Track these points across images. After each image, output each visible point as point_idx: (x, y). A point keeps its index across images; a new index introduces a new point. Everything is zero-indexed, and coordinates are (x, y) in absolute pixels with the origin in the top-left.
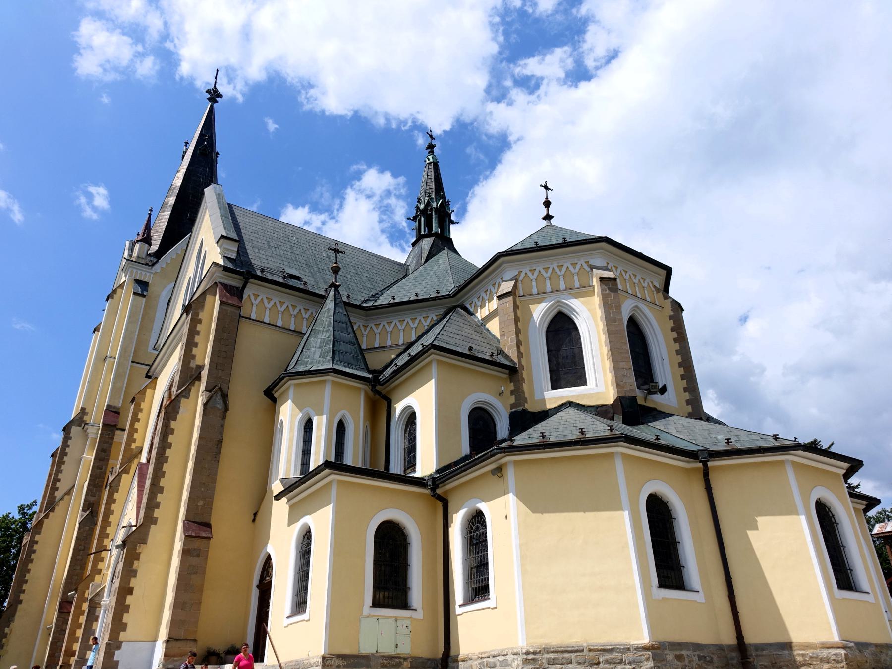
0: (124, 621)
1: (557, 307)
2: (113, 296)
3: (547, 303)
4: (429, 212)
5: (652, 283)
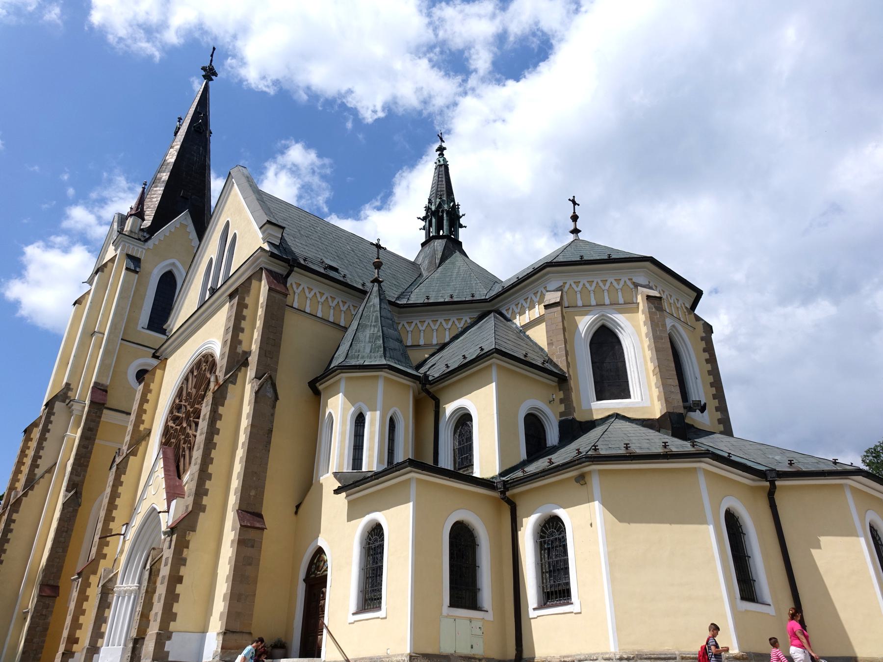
0: (174, 610)
1: (601, 320)
2: (103, 269)
3: (592, 316)
4: (440, 214)
5: (684, 304)
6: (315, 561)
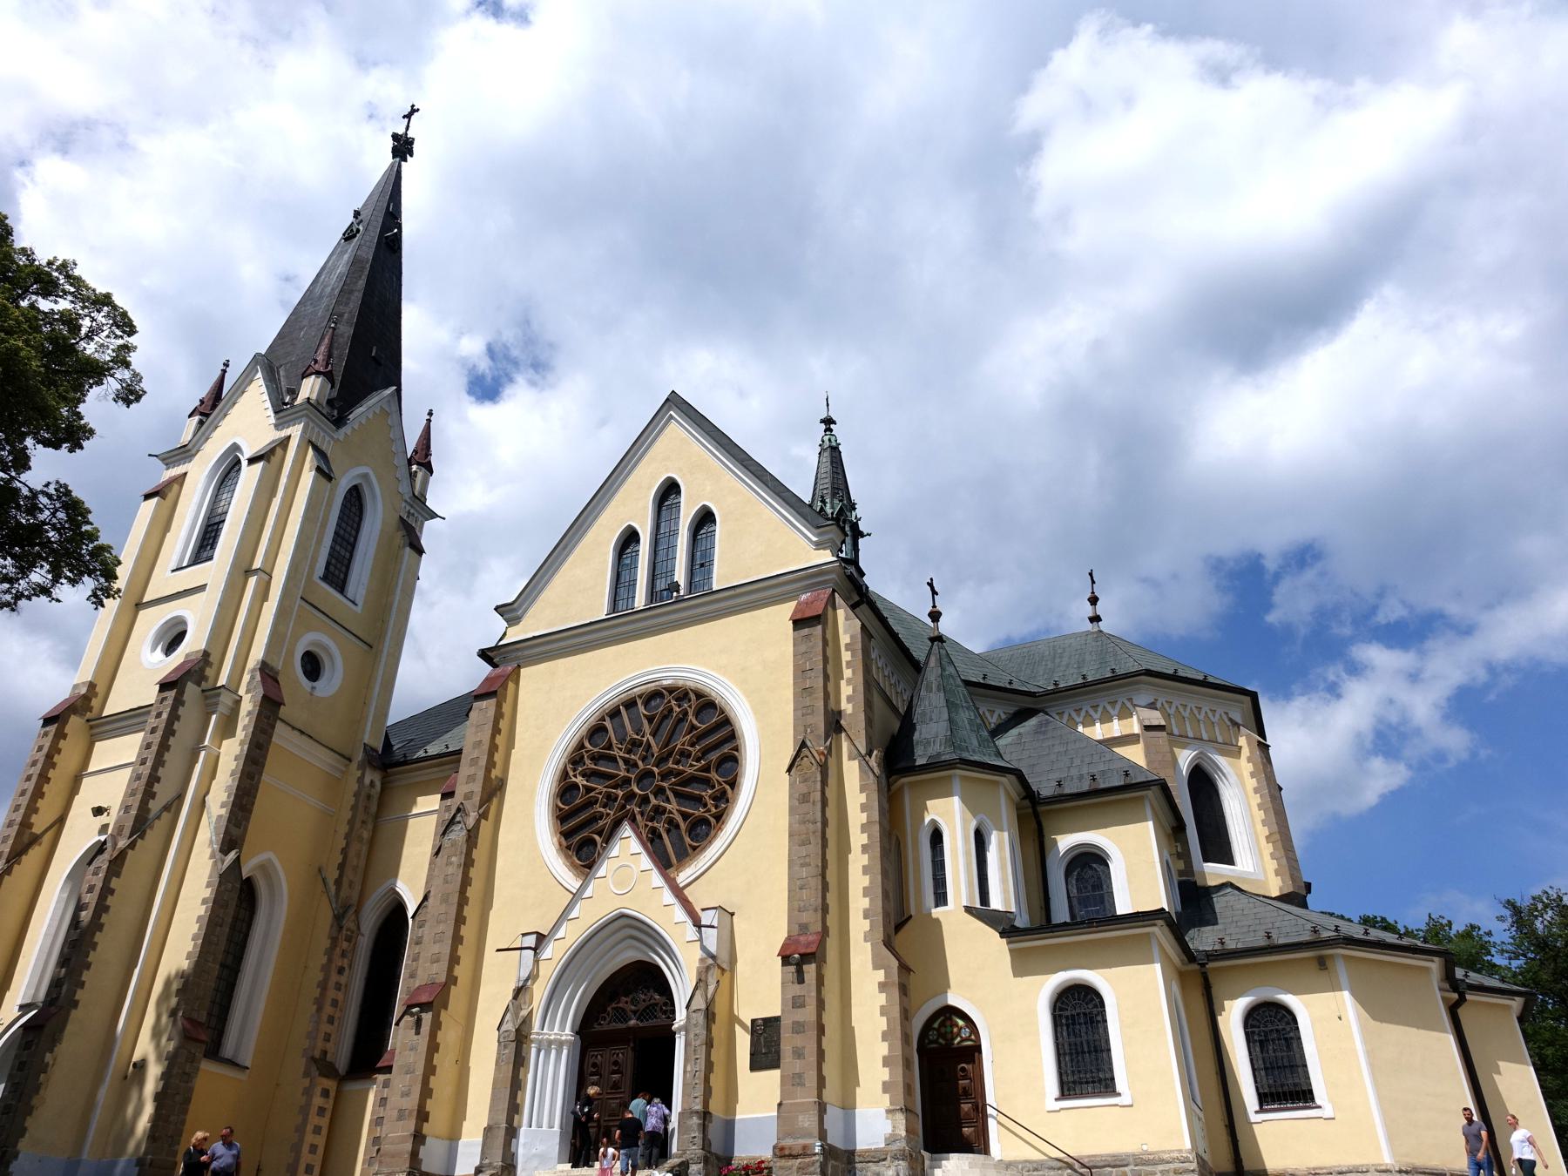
6: (936, 1025)
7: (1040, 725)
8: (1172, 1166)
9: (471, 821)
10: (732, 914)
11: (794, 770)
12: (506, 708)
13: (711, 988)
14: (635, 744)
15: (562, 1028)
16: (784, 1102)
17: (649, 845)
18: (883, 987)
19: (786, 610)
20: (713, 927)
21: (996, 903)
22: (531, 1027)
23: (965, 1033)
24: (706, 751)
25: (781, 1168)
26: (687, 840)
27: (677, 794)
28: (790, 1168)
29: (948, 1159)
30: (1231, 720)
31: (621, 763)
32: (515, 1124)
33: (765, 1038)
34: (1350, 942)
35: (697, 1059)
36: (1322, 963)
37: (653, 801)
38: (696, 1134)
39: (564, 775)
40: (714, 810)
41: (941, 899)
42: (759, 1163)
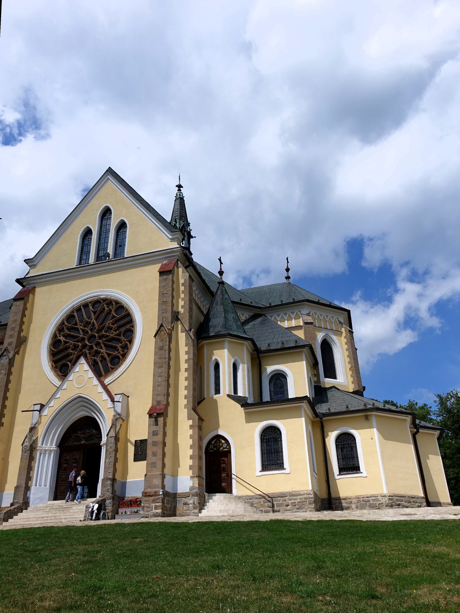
7: (263, 321)
8: (304, 496)
9: (11, 355)
10: (128, 397)
11: (157, 336)
12: (28, 305)
13: (118, 428)
14: (88, 323)
15: (51, 444)
16: (148, 474)
17: (92, 367)
18: (191, 427)
19: (157, 267)
20: (119, 402)
21: (240, 393)
22: (37, 444)
23: (225, 446)
24: (119, 327)
25: (145, 501)
26: (109, 365)
27: (105, 345)
28: (149, 500)
29: (215, 496)
30: (339, 321)
31: (81, 331)
32: (29, 485)
33: (141, 448)
34: (378, 409)
35: (111, 457)
36: (367, 418)
37: (95, 348)
38: (110, 488)
39: (55, 336)
40: (122, 353)
41: (217, 391)
42: (136, 499)
